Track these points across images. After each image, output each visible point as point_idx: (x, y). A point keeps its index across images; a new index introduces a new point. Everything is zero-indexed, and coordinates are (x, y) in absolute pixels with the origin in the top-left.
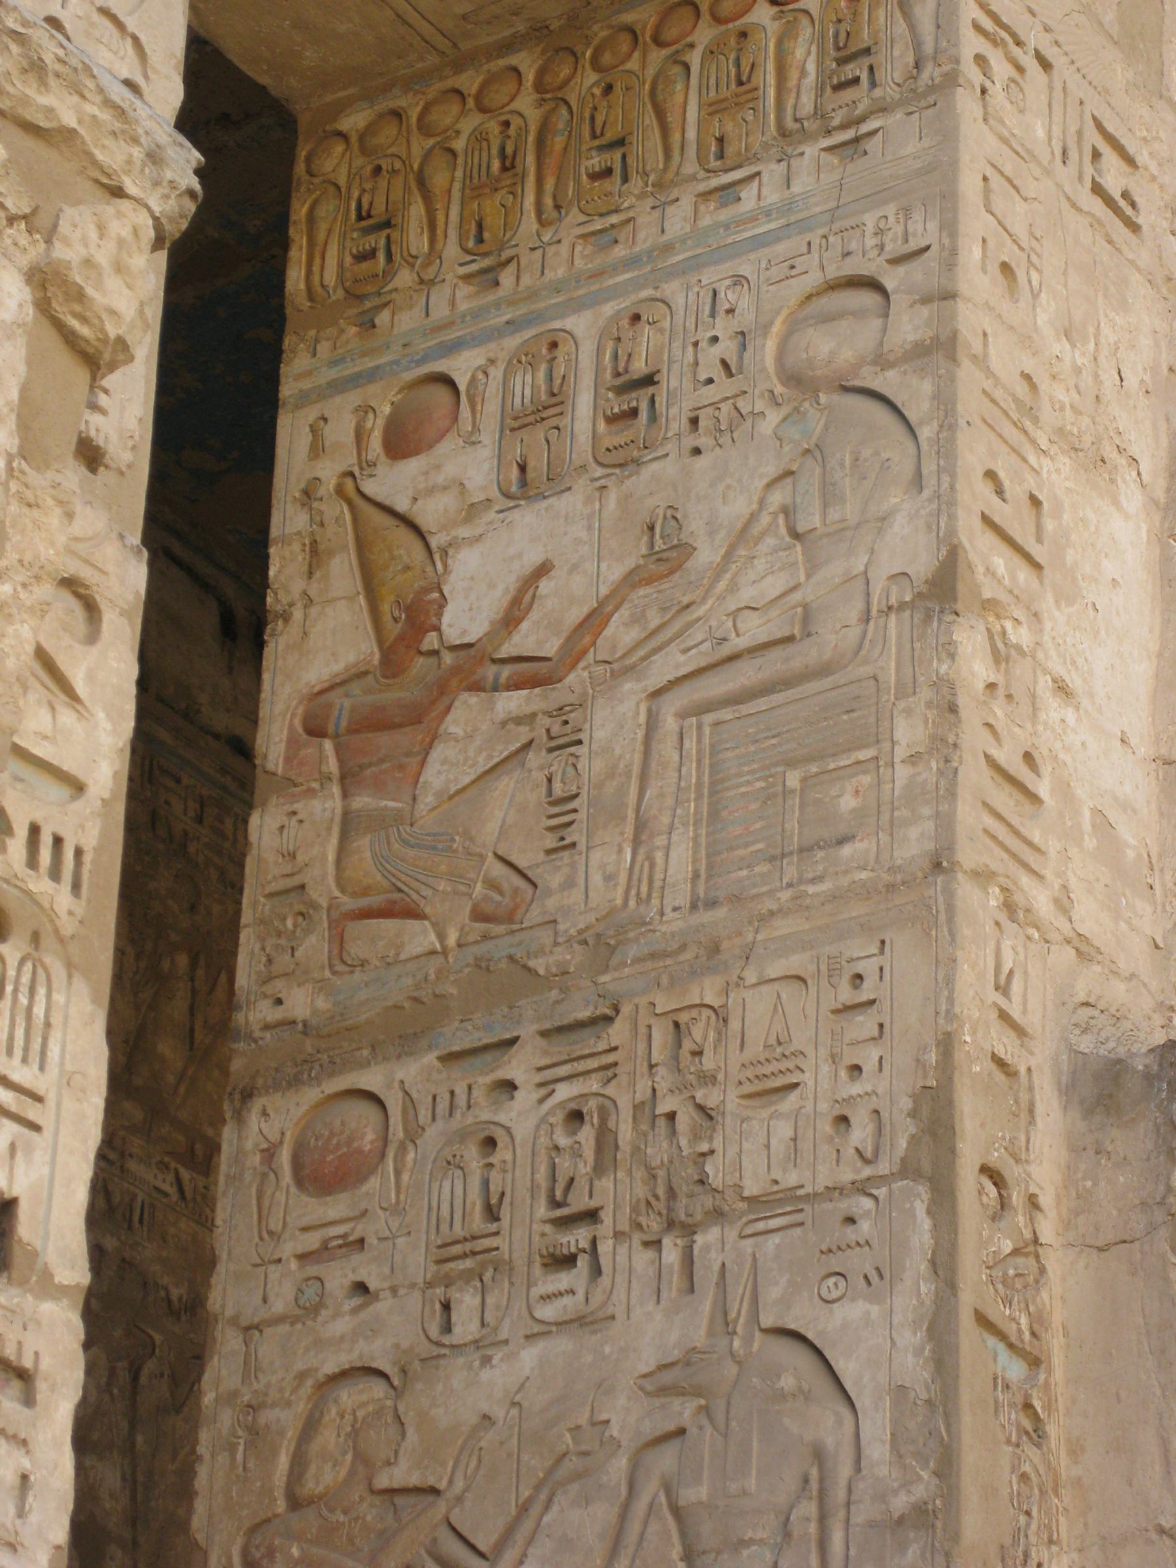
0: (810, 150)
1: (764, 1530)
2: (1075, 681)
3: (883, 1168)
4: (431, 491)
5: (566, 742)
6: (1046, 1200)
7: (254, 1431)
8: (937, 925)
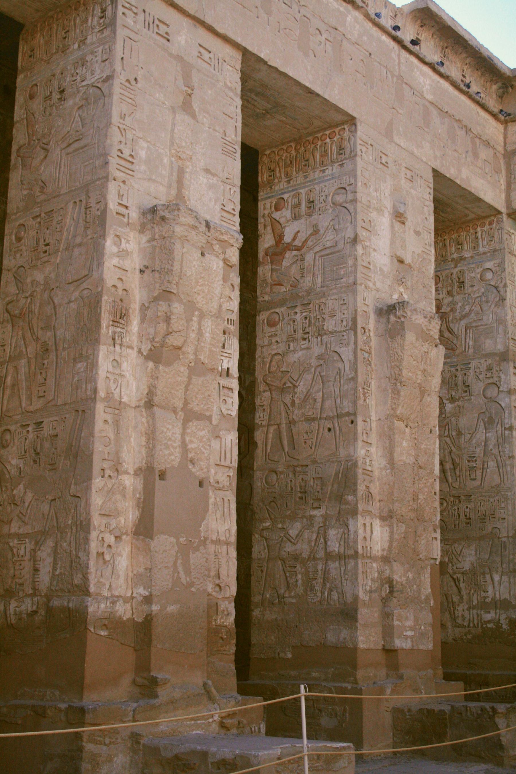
0: (336, 165)
1: (332, 379)
2: (377, 248)
3: (348, 328)
4: (282, 217)
5: (302, 260)
6: (371, 330)
7: (263, 361)
8: (354, 292)
